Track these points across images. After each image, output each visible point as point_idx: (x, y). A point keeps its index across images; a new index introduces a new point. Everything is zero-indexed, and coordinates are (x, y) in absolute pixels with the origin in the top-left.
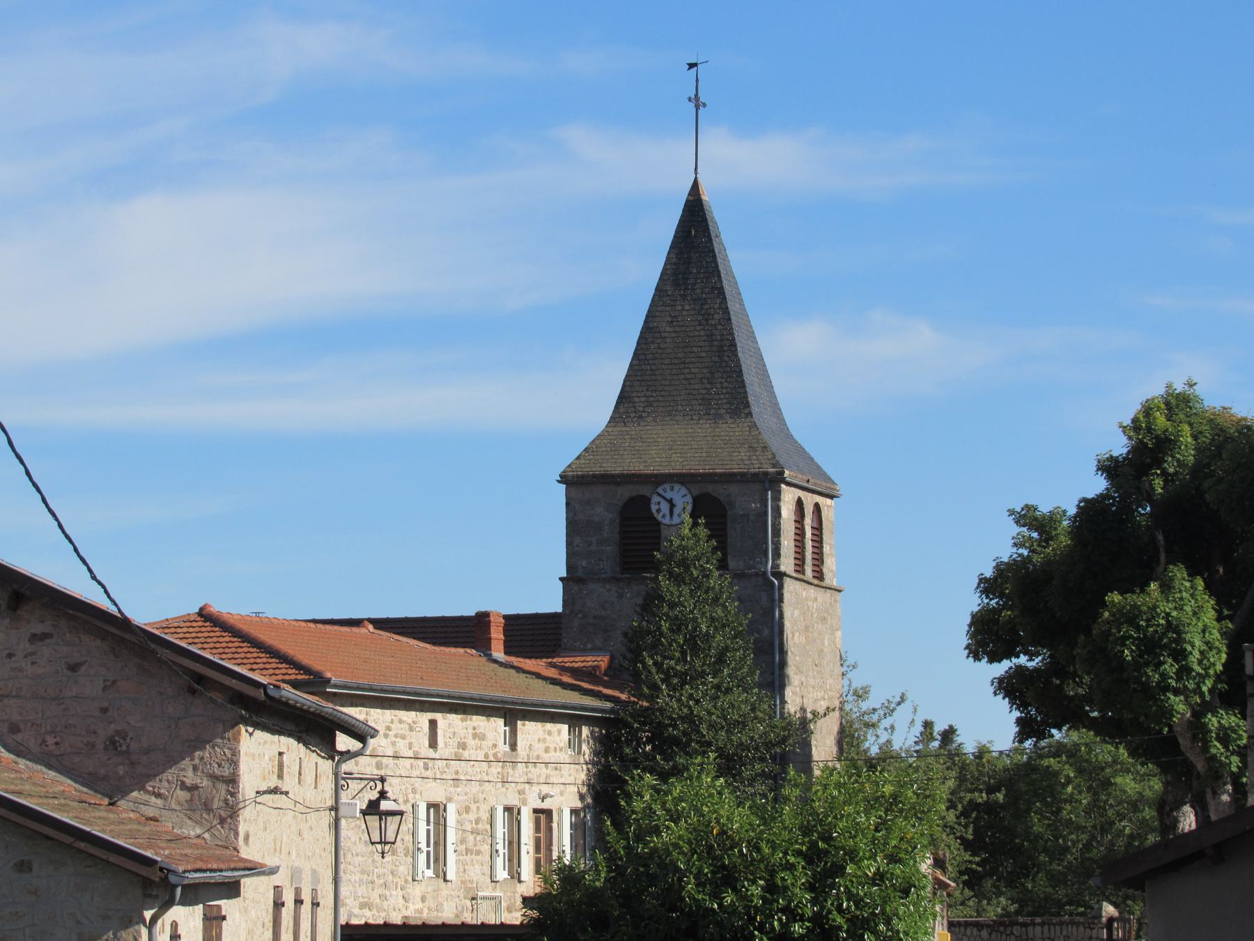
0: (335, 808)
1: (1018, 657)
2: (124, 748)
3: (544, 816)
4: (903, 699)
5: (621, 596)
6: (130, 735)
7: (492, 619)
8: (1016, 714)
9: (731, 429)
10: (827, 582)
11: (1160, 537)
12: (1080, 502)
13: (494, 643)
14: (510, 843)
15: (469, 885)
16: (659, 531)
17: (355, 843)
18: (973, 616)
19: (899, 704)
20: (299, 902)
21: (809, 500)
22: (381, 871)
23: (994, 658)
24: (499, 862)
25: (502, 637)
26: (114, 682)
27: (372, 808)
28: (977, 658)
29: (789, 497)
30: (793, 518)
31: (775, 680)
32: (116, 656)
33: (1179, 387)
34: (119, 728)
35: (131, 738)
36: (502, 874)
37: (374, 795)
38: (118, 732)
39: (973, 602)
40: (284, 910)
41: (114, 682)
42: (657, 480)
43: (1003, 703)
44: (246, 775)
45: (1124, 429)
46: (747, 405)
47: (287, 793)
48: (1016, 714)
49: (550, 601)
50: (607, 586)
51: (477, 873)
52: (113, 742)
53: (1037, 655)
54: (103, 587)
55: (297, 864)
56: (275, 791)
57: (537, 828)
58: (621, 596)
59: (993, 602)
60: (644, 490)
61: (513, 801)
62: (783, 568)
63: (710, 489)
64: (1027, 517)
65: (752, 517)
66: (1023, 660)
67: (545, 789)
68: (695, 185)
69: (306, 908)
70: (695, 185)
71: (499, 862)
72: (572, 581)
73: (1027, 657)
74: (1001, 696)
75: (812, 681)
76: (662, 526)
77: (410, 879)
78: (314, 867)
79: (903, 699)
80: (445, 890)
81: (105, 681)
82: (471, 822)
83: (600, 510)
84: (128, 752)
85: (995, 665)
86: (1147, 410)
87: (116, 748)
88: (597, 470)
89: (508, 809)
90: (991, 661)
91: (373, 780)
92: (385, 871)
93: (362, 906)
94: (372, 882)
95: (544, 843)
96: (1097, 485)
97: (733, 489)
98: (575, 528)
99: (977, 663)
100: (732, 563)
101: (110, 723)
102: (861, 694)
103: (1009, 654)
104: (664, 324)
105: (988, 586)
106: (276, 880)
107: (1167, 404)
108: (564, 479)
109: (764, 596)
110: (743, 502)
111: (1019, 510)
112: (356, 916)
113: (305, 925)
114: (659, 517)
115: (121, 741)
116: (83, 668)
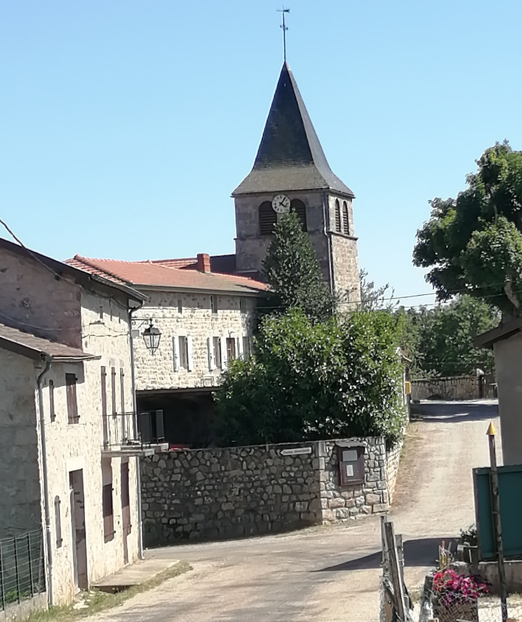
0: (130, 333)
1: (435, 263)
2: (28, 306)
3: (230, 341)
4: (387, 286)
5: (261, 245)
6: (31, 300)
7: (204, 257)
8: (436, 289)
9: (306, 170)
10: (351, 235)
11: (495, 208)
12: (459, 194)
13: (206, 268)
14: (217, 353)
15: (199, 372)
16: (276, 216)
17: (147, 355)
18: (416, 249)
19: (385, 289)
20: (113, 374)
21: (341, 201)
22: (159, 367)
23: (425, 265)
24: (212, 361)
25: (209, 264)
26: (22, 276)
27: (148, 332)
28: (418, 265)
29: (332, 200)
30: (335, 208)
31: (329, 278)
32: (22, 264)
33: (501, 143)
34: (26, 297)
35: (31, 302)
36: (214, 367)
37: (148, 327)
38: (25, 299)
39: (415, 242)
40: (106, 377)
41: (22, 276)
42: (275, 194)
43: (430, 285)
44: (85, 316)
45: (478, 163)
46: (312, 160)
47: (104, 324)
48: (436, 289)
49: (230, 249)
50: (255, 241)
51: (203, 367)
52: (23, 303)
53: (444, 261)
54: (5, 225)
55: (112, 357)
56: (99, 322)
57: (228, 347)
58: (261, 245)
59: (424, 241)
60: (269, 198)
61: (217, 334)
62: (331, 230)
63: (298, 196)
64: (437, 203)
65: (316, 208)
66: (437, 265)
67: (231, 330)
68: (285, 65)
69: (118, 377)
70: (285, 65)
71: (212, 361)
72: (240, 239)
73: (439, 264)
74: (429, 282)
75: (346, 278)
76: (278, 214)
77: (173, 370)
78: (121, 358)
79: (387, 286)
80: (189, 375)
81: (18, 276)
82: (198, 344)
83: (250, 208)
84: (30, 308)
85: (426, 268)
86: (488, 153)
87: (24, 306)
88: (248, 190)
89: (215, 338)
90: (424, 266)
91: (147, 320)
92: (161, 367)
93: (152, 382)
94: (156, 372)
95: (231, 353)
96: (466, 187)
97: (308, 196)
98: (240, 216)
99: (418, 268)
100: (309, 229)
101: (21, 295)
102: (371, 286)
103: (432, 262)
104: (273, 126)
105: (421, 235)
106: (102, 362)
107: (497, 150)
108: (234, 195)
109: (324, 243)
110: (313, 201)
111: (433, 200)
112: (150, 387)
113: (118, 384)
114: (276, 210)
115: (27, 303)
116: (8, 271)
